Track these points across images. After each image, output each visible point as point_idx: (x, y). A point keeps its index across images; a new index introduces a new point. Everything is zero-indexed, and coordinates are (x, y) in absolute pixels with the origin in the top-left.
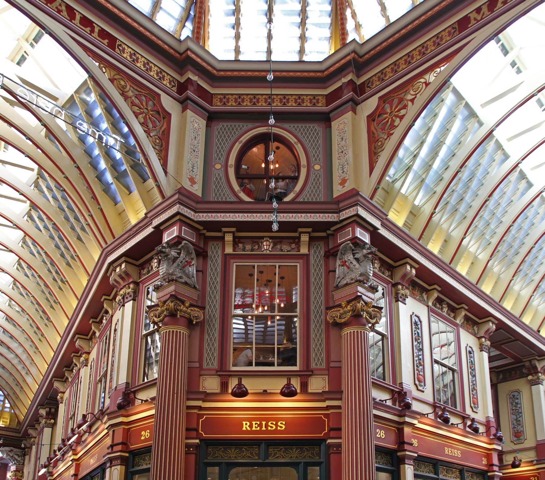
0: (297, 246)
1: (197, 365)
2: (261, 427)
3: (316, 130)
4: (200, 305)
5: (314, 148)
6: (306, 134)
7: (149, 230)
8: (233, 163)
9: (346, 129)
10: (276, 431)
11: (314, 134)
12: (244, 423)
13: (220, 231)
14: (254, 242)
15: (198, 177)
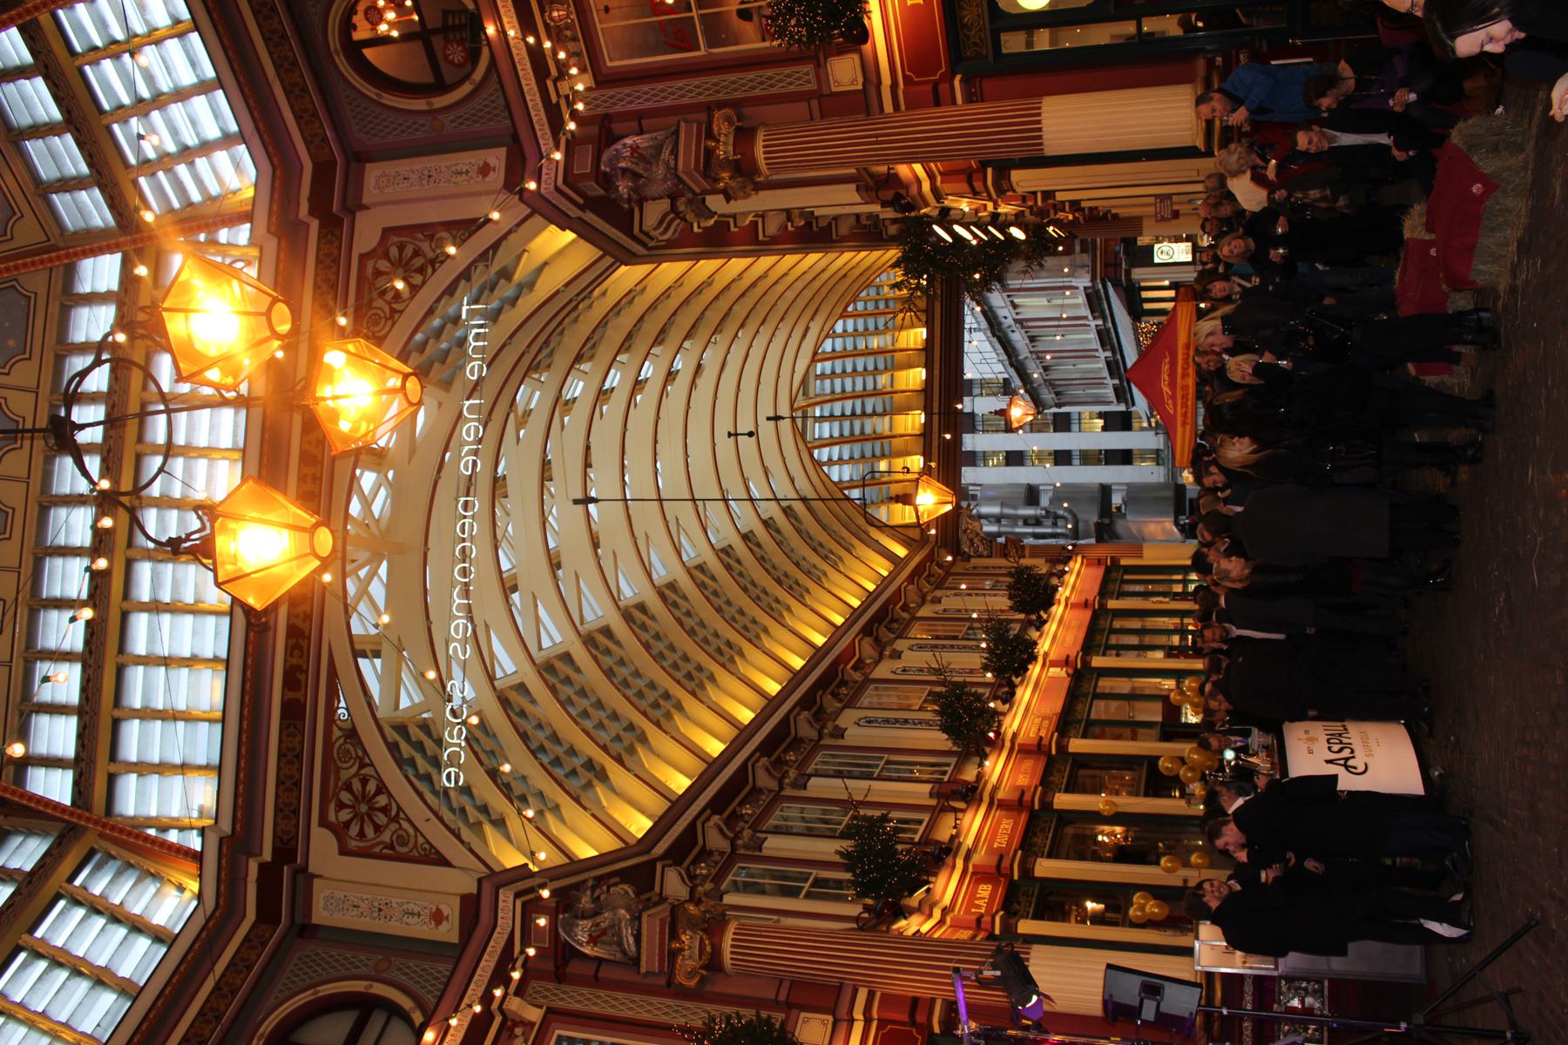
1: (814, 103)
7: (590, 217)
15: (473, 161)
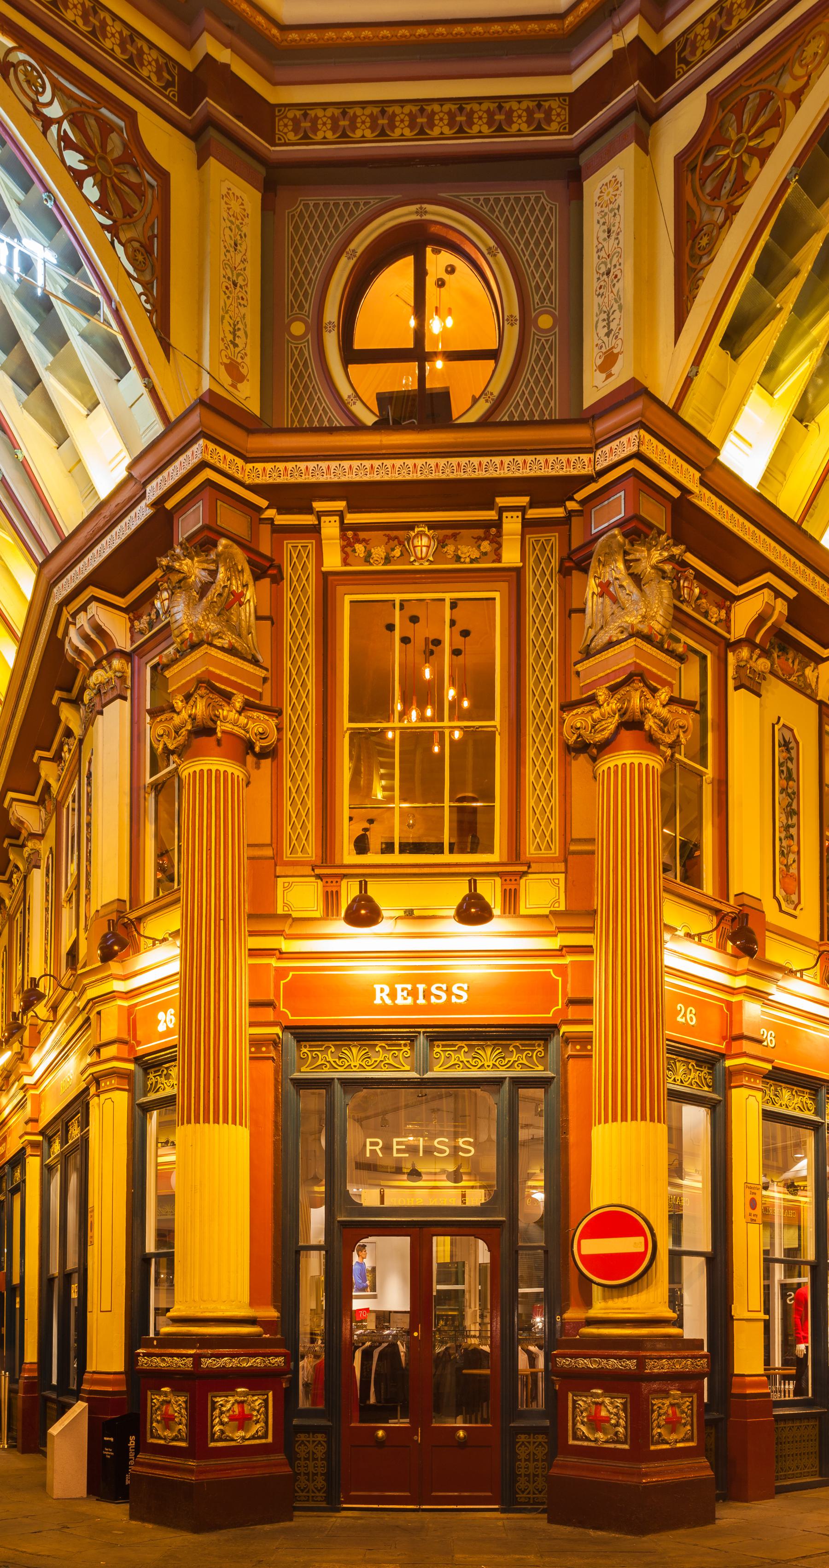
0: (496, 546)
2: (416, 998)
3: (543, 208)
4: (266, 701)
5: (537, 265)
6: (517, 221)
8: (334, 319)
9: (620, 201)
10: (449, 1007)
11: (537, 221)
12: (377, 987)
13: (309, 510)
14: (390, 538)
